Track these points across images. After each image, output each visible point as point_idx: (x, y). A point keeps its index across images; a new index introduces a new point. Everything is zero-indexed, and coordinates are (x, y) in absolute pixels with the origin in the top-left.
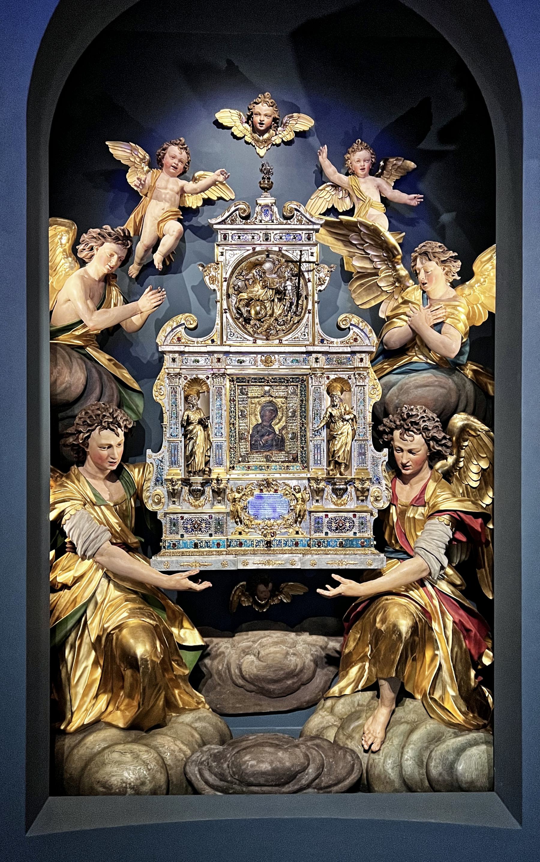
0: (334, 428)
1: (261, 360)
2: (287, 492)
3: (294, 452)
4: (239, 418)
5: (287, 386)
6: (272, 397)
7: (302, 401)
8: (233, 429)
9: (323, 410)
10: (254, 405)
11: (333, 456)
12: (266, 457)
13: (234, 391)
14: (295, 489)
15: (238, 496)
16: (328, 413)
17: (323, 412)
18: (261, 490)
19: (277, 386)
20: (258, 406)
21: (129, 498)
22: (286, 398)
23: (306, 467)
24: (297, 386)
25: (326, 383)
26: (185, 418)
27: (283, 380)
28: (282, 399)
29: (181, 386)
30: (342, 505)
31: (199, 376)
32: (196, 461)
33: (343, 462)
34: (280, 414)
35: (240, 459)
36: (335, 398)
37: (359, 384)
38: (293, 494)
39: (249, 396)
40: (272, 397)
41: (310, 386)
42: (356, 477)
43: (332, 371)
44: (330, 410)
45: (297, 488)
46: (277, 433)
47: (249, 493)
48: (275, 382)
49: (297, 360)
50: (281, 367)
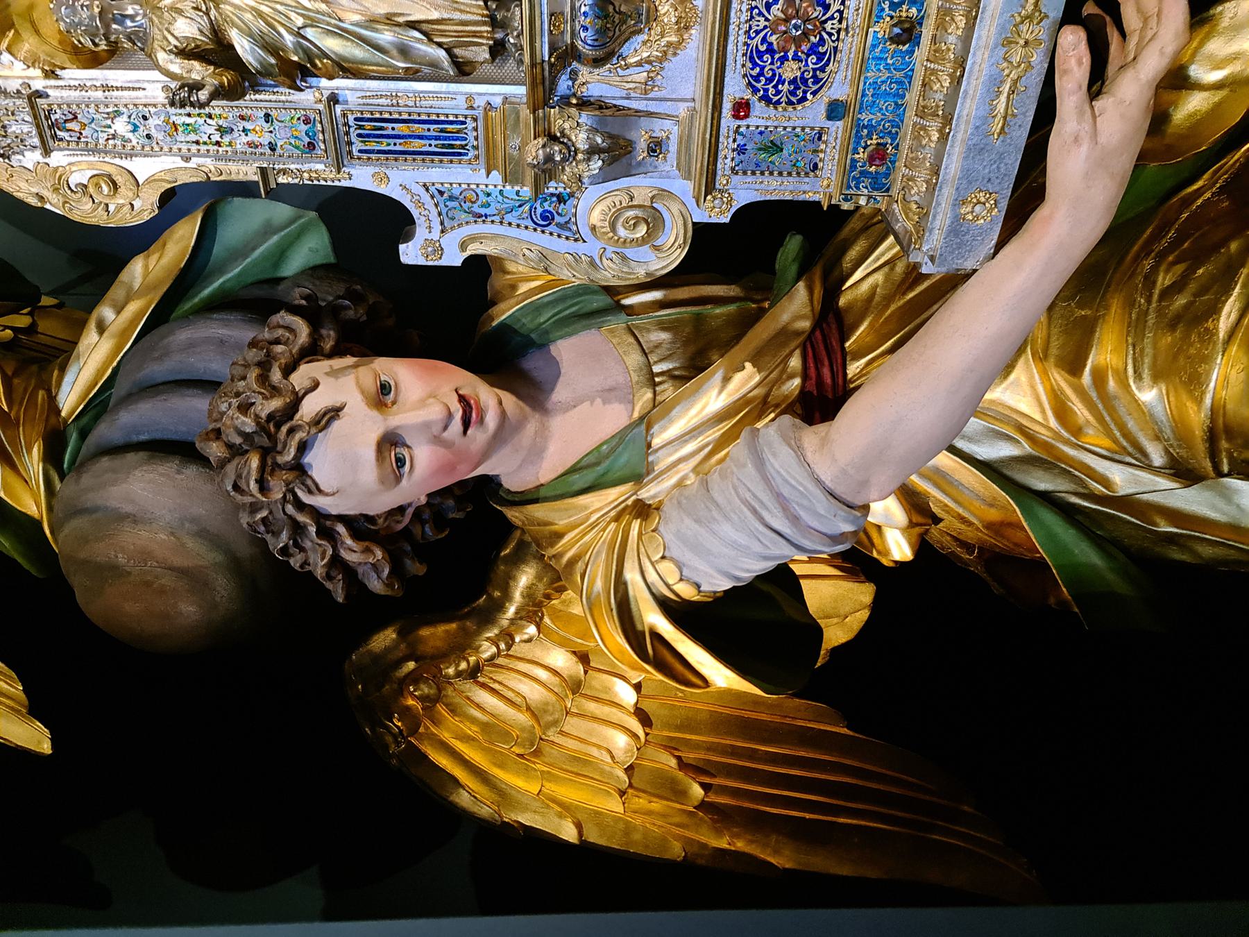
21: (623, 317)
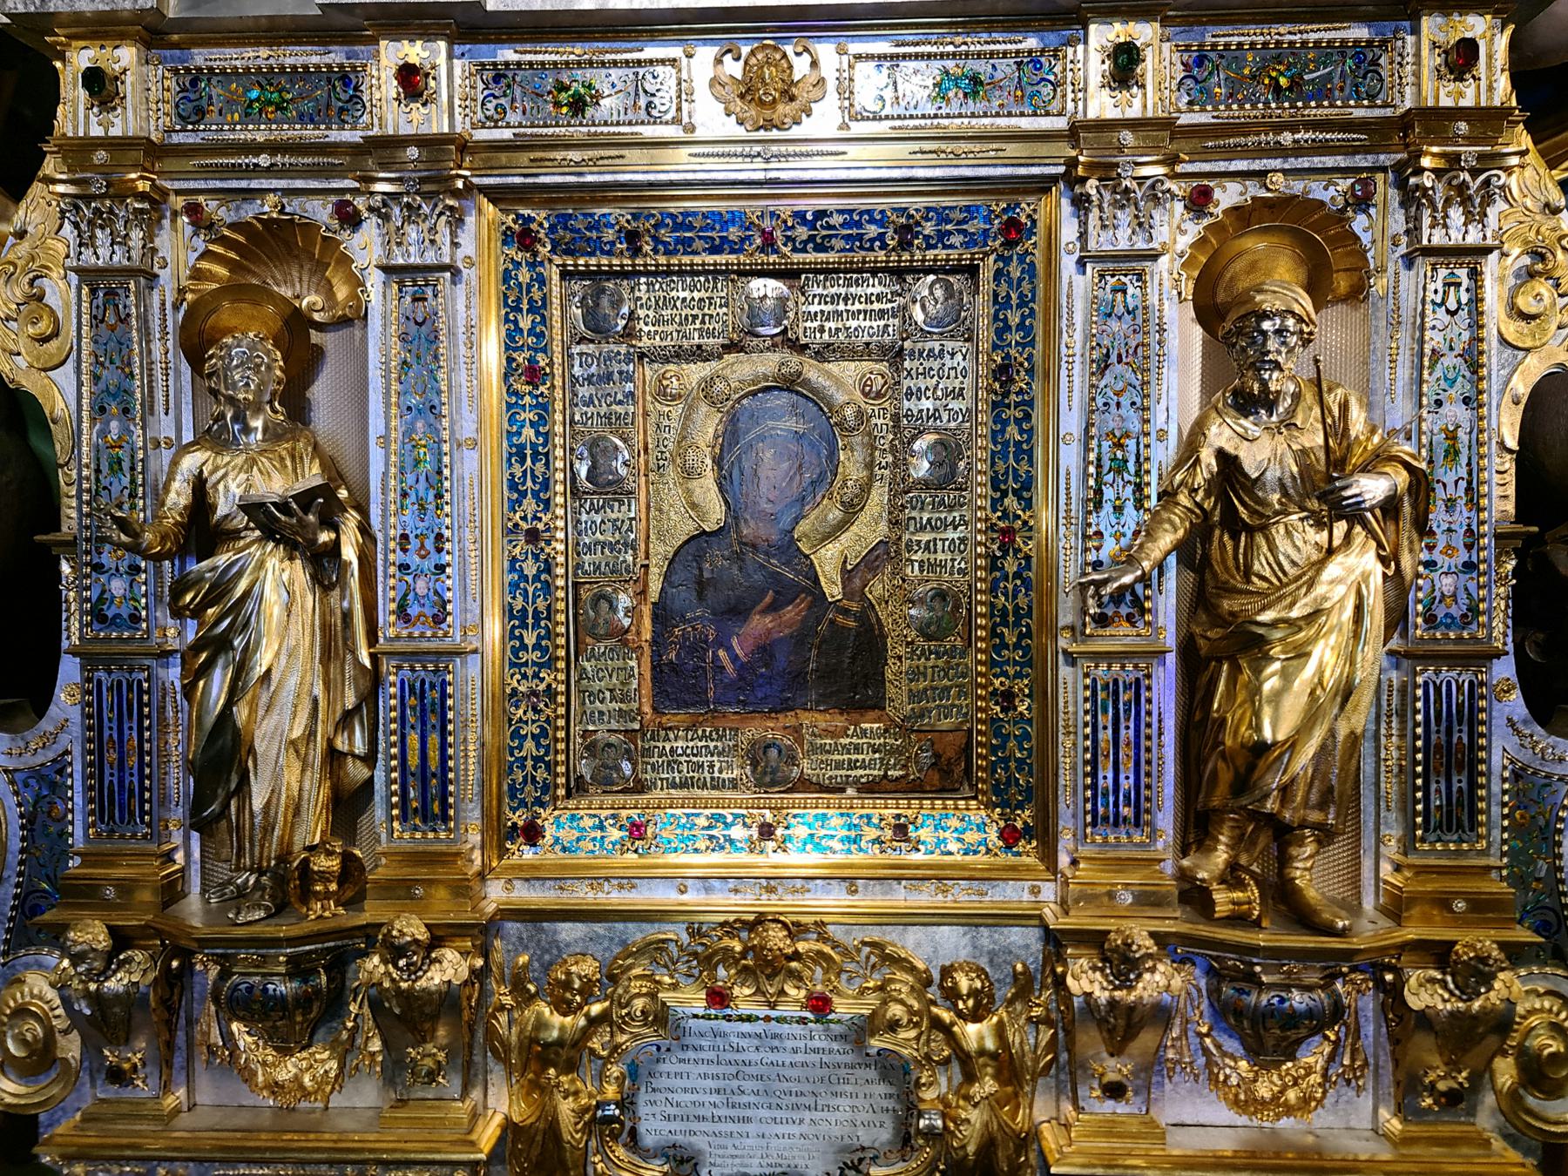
0: (1248, 573)
1: (715, 82)
2: (896, 1010)
3: (946, 724)
4: (575, 492)
5: (899, 273)
6: (802, 349)
7: (1003, 372)
8: (530, 569)
9: (1162, 435)
10: (677, 410)
11: (1244, 783)
12: (756, 755)
13: (539, 309)
14: (952, 995)
15: (558, 1023)
16: (1207, 457)
17: (1163, 454)
18: (718, 998)
19: (828, 271)
20: (704, 408)
22: (895, 355)
23: (1028, 833)
24: (972, 271)
25: (1184, 242)
26: (179, 496)
27: (872, 230)
28: (866, 366)
29: (165, 275)
30: (1289, 1110)
31: (294, 206)
32: (258, 803)
33: (1315, 816)
34: (852, 466)
35: (584, 768)
36: (1272, 344)
37: (1438, 238)
38: (937, 1023)
39: (645, 343)
40: (802, 349)
41: (1068, 264)
42: (1410, 933)
43: (1231, 153)
44: (1220, 435)
45: (964, 984)
46: (833, 590)
47: (639, 1004)
48: (820, 248)
49: (975, 80)
50: (859, 128)
